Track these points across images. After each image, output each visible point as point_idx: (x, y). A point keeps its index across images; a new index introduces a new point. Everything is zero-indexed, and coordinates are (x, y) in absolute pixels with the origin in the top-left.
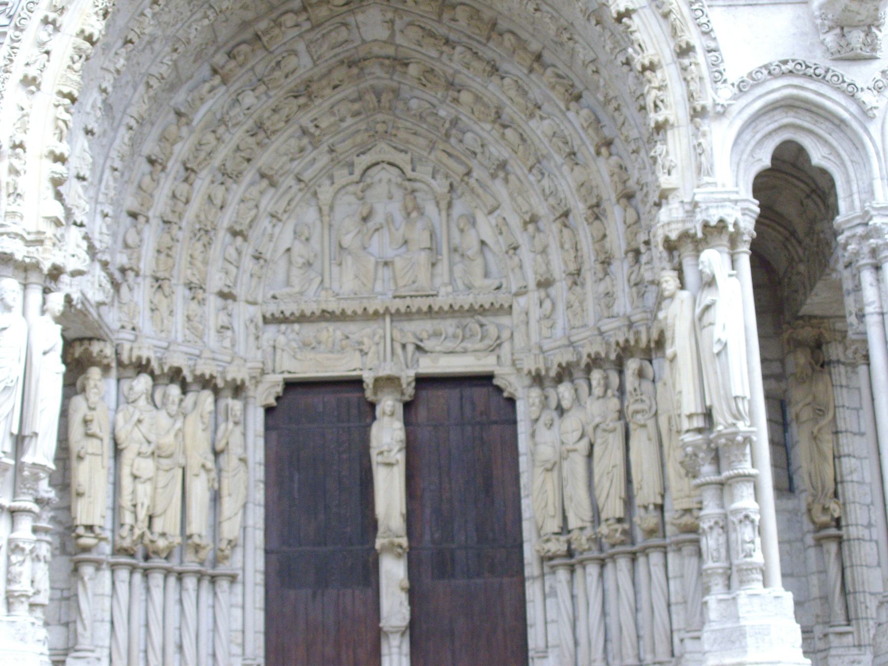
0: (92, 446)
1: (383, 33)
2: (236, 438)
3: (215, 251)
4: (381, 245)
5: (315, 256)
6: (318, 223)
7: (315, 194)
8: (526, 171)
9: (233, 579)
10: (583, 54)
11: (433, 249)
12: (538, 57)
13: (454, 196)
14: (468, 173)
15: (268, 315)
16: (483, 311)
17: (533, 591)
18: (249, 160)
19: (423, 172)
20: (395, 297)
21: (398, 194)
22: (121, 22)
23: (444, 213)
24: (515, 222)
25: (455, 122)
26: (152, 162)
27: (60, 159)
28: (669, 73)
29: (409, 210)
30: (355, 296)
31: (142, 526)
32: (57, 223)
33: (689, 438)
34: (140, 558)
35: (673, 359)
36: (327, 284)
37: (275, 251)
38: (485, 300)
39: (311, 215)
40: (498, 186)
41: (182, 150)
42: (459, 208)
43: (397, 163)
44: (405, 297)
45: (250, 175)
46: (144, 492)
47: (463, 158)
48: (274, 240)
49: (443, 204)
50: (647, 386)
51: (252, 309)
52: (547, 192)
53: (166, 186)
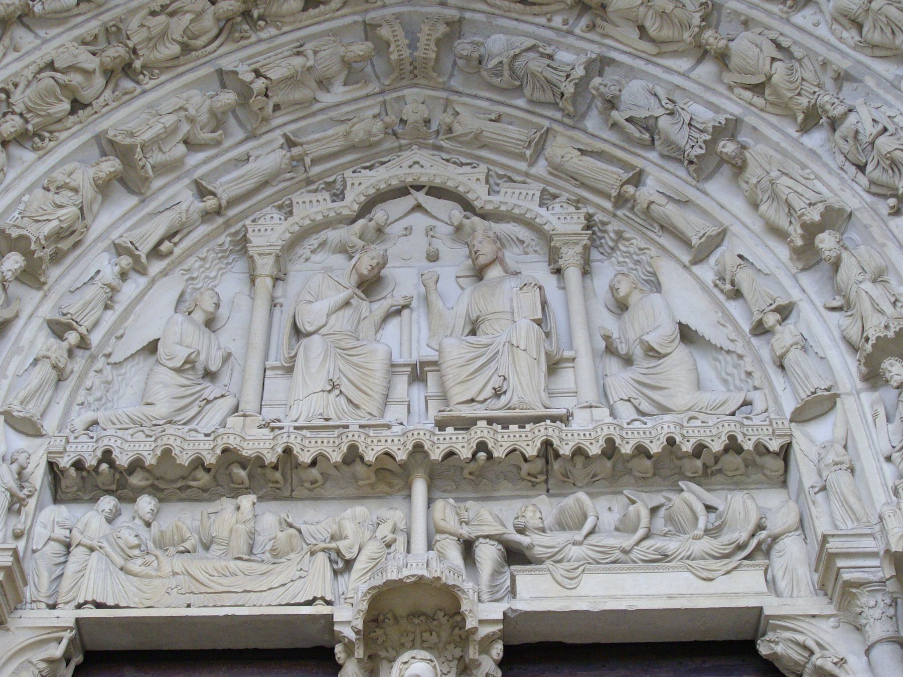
5: (227, 357)
6: (244, 302)
7: (242, 243)
8: (792, 131)
13: (595, 254)
14: (637, 179)
15: (65, 462)
18: (77, 105)
19: (520, 199)
20: (441, 425)
23: (573, 274)
24: (774, 257)
25: (599, 65)
29: (482, 260)
36: (249, 404)
37: (116, 334)
39: (231, 285)
43: (450, 184)
44: (473, 422)
45: (73, 140)
47: (620, 154)
48: (119, 308)
49: (570, 257)
51: (19, 442)
52: (869, 130)
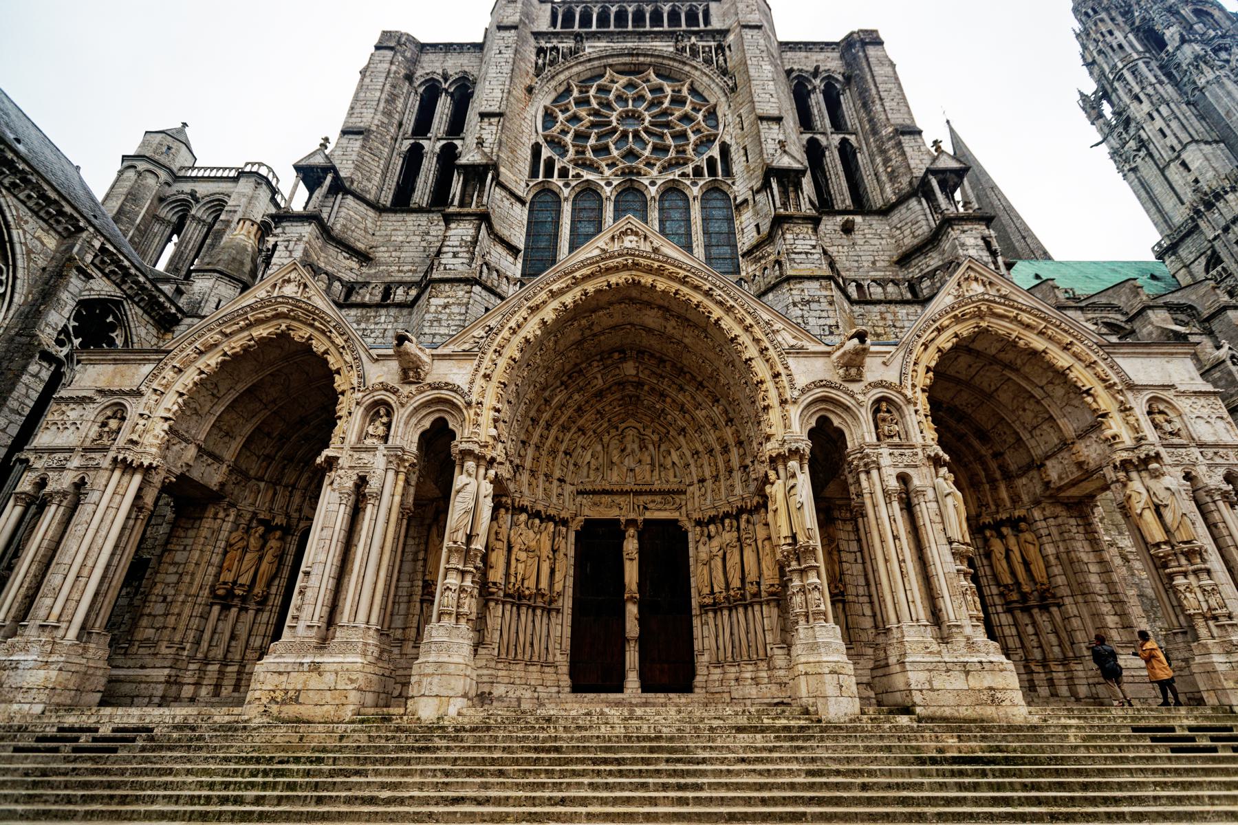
0: (499, 544)
1: (634, 372)
2: (563, 545)
3: (558, 461)
4: (629, 462)
9: (558, 611)
10: (723, 381)
11: (652, 464)
12: (701, 384)
16: (674, 492)
17: (696, 622)
19: (648, 432)
21: (637, 440)
22: (526, 357)
24: (688, 454)
25: (663, 411)
26: (532, 419)
27: (498, 411)
28: (769, 384)
30: (618, 483)
31: (519, 583)
32: (494, 438)
33: (785, 548)
34: (517, 599)
35: (775, 511)
38: (675, 487)
39: (599, 448)
40: (681, 438)
41: (546, 416)
42: (663, 448)
45: (573, 431)
46: (521, 566)
50: (750, 527)
53: (538, 431)
